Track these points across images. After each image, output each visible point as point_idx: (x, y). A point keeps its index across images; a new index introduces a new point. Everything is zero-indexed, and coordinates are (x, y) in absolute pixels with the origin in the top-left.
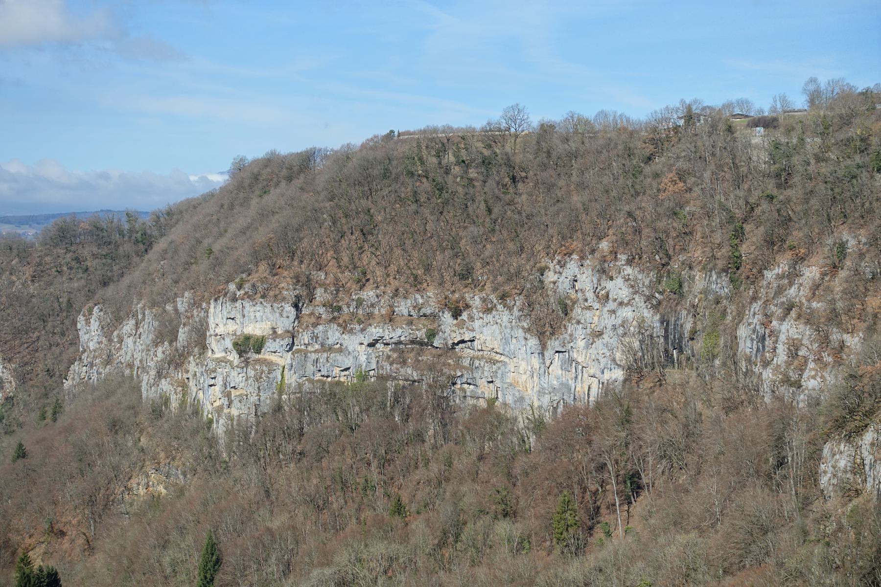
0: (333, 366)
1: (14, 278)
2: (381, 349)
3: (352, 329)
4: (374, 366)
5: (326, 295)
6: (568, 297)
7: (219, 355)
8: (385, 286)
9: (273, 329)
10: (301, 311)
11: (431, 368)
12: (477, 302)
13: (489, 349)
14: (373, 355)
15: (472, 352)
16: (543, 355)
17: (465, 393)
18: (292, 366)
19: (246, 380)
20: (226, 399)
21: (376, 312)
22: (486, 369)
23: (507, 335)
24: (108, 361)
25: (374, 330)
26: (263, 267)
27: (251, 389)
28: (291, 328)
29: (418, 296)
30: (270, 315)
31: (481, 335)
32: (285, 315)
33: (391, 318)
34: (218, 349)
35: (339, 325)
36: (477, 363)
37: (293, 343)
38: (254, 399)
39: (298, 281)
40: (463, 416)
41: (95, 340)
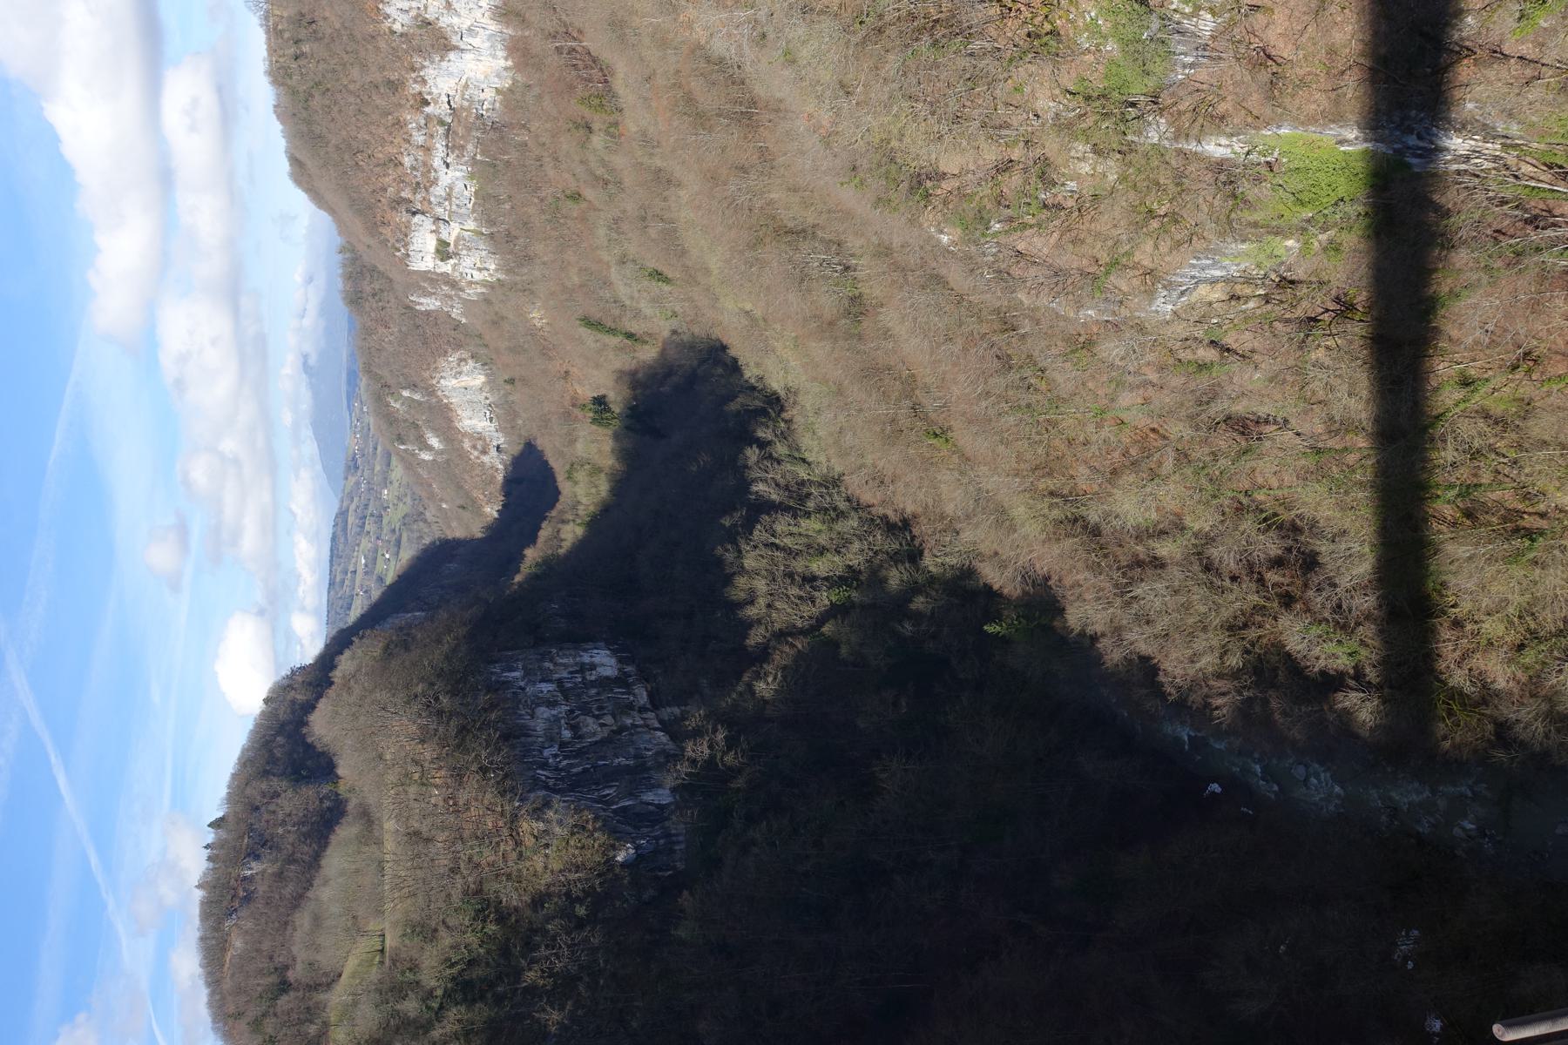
0: (462, 196)
4: (465, 168)
6: (416, 18)
11: (469, 130)
12: (417, 88)
16: (462, 50)
29: (410, 126)
33: (427, 149)
34: (446, 267)
35: (431, 186)
36: (466, 97)
37: (443, 220)
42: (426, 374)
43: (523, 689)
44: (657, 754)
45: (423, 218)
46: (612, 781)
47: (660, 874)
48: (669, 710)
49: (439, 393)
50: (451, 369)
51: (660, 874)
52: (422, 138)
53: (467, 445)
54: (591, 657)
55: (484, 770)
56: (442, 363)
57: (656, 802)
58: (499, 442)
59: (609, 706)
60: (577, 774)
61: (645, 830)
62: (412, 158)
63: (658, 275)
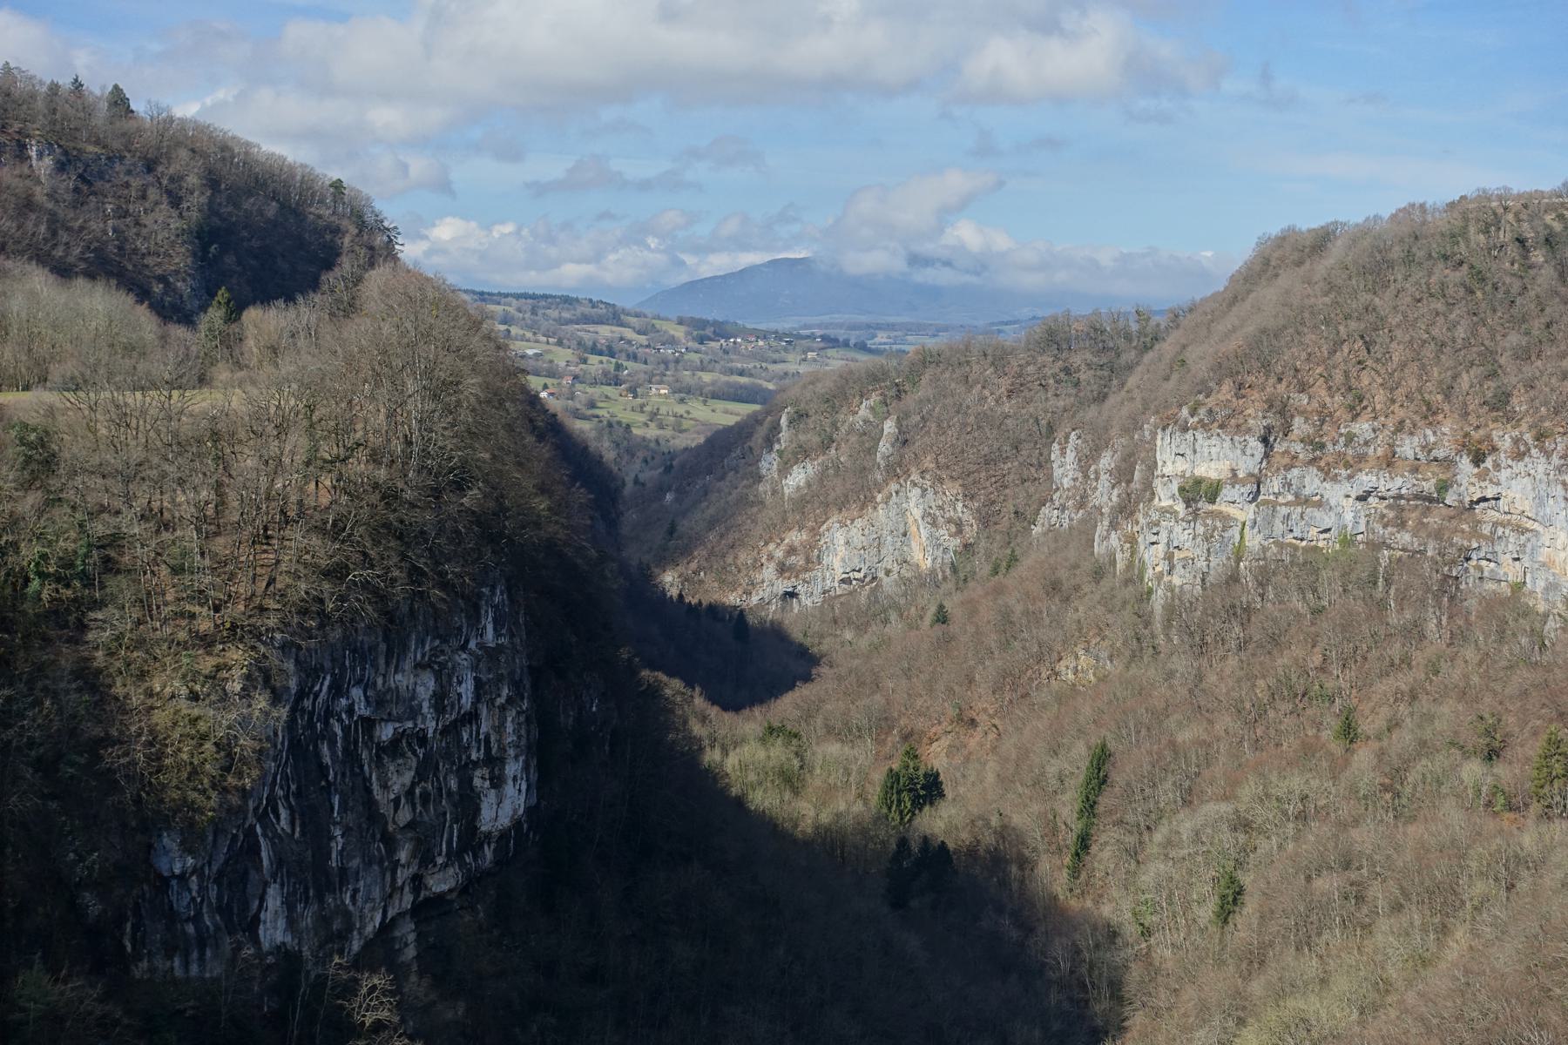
1: (987, 393)
2: (1374, 505)
3: (1336, 475)
4: (1362, 528)
5: (1307, 426)
7: (1166, 503)
8: (1386, 417)
9: (1233, 471)
10: (1272, 447)
11: (1438, 535)
12: (1506, 444)
13: (1518, 512)
14: (1363, 514)
15: (1497, 514)
17: (1482, 573)
18: (1255, 523)
19: (1194, 539)
20: (1167, 562)
21: (1371, 451)
22: (1511, 540)
23: (1542, 492)
24: (1081, 505)
25: (1365, 478)
26: (1227, 385)
27: (1198, 551)
28: (1256, 471)
29: (1429, 432)
30: (1229, 452)
31: (1509, 491)
32: (1249, 452)
33: (1389, 462)
34: (1166, 496)
35: (1320, 469)
36: (1500, 531)
38: (1201, 564)
39: (1271, 406)
40: (1472, 603)
41: (1070, 476)
42: (928, 462)
43: (464, 648)
44: (347, 915)
45: (1259, 456)
46: (303, 825)
47: (129, 926)
48: (411, 937)
49: (893, 487)
50: (941, 508)
51: (129, 926)
52: (1410, 455)
53: (795, 537)
54: (515, 779)
55: (336, 573)
56: (952, 489)
57: (262, 916)
58: (802, 597)
59: (429, 816)
60: (317, 754)
61: (213, 893)
62: (1369, 435)
63: (1231, 900)
